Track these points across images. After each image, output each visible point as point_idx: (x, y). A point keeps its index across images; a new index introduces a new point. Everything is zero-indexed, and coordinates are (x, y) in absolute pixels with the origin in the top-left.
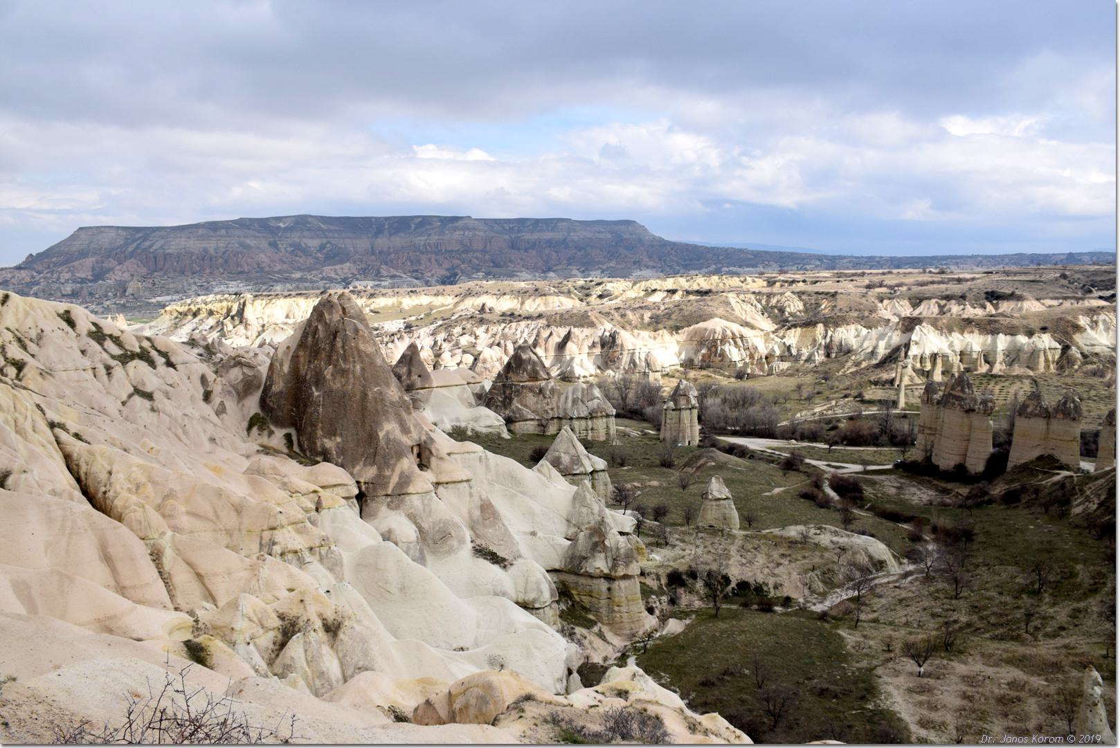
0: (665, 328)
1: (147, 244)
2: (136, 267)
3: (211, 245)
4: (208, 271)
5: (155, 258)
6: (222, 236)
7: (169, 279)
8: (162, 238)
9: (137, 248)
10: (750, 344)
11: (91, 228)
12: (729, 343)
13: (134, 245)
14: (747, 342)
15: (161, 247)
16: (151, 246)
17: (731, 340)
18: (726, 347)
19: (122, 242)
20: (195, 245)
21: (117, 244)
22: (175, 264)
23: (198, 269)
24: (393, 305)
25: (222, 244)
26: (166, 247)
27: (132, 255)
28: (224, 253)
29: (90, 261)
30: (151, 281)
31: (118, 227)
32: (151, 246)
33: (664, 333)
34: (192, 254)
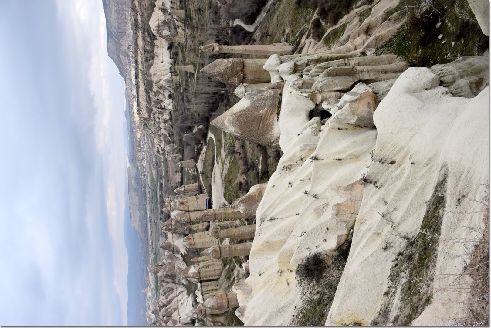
0: (153, 40)
1: (114, 33)
2: (124, 40)
3: (113, 8)
4: (125, 12)
5: (119, 32)
6: (109, 2)
7: (129, 38)
8: (111, 27)
9: (116, 38)
10: (161, 24)
11: (108, 52)
12: (160, 33)
13: (115, 38)
14: (161, 25)
15: (115, 28)
16: (115, 32)
17: (160, 31)
18: (163, 35)
19: (113, 41)
20: (114, 16)
21: (114, 43)
22: (122, 25)
23: (124, 16)
24: (142, 74)
25: (113, 3)
26: (115, 27)
27: (119, 40)
28: (117, 3)
29: (122, 57)
30: (130, 46)
31: (107, 41)
32: (115, 32)
33: (155, 42)
34: (117, 17)
